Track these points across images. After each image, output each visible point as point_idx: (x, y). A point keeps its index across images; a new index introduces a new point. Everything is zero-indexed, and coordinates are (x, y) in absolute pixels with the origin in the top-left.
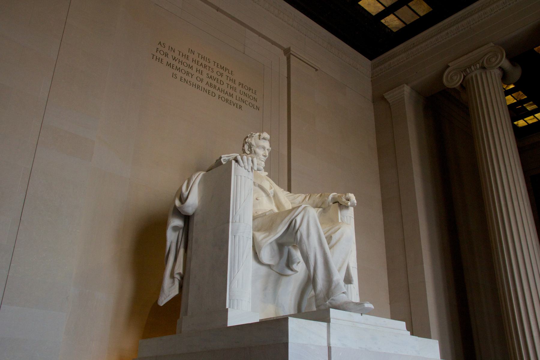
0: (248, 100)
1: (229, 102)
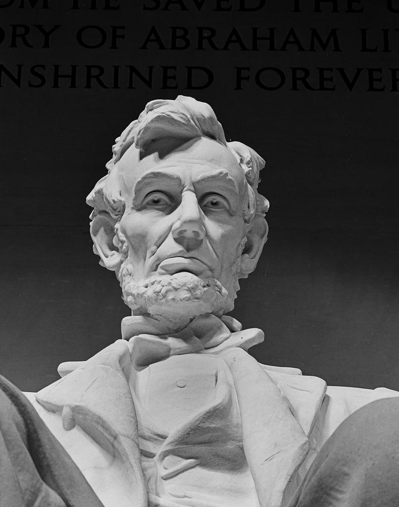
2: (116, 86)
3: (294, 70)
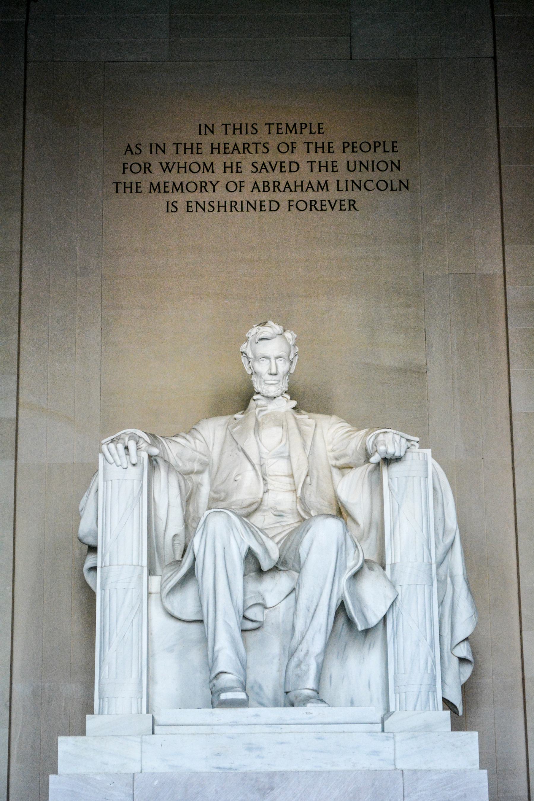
0: (376, 176)
1: (318, 206)
2: (242, 211)
3: (311, 201)
